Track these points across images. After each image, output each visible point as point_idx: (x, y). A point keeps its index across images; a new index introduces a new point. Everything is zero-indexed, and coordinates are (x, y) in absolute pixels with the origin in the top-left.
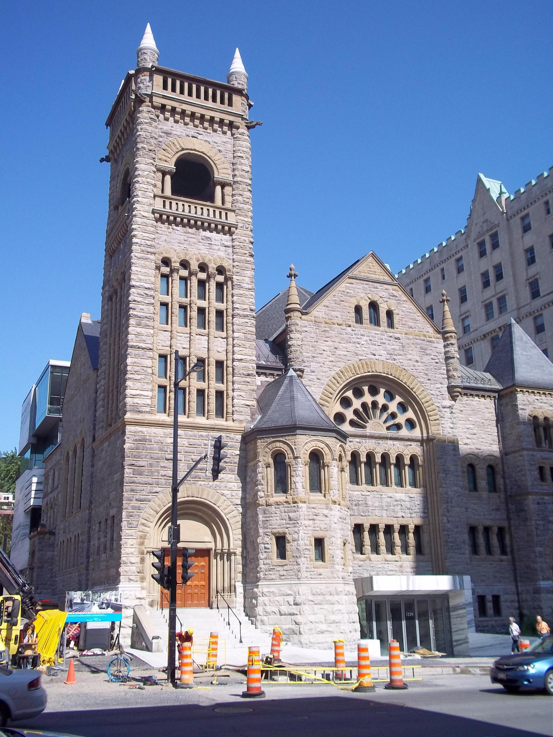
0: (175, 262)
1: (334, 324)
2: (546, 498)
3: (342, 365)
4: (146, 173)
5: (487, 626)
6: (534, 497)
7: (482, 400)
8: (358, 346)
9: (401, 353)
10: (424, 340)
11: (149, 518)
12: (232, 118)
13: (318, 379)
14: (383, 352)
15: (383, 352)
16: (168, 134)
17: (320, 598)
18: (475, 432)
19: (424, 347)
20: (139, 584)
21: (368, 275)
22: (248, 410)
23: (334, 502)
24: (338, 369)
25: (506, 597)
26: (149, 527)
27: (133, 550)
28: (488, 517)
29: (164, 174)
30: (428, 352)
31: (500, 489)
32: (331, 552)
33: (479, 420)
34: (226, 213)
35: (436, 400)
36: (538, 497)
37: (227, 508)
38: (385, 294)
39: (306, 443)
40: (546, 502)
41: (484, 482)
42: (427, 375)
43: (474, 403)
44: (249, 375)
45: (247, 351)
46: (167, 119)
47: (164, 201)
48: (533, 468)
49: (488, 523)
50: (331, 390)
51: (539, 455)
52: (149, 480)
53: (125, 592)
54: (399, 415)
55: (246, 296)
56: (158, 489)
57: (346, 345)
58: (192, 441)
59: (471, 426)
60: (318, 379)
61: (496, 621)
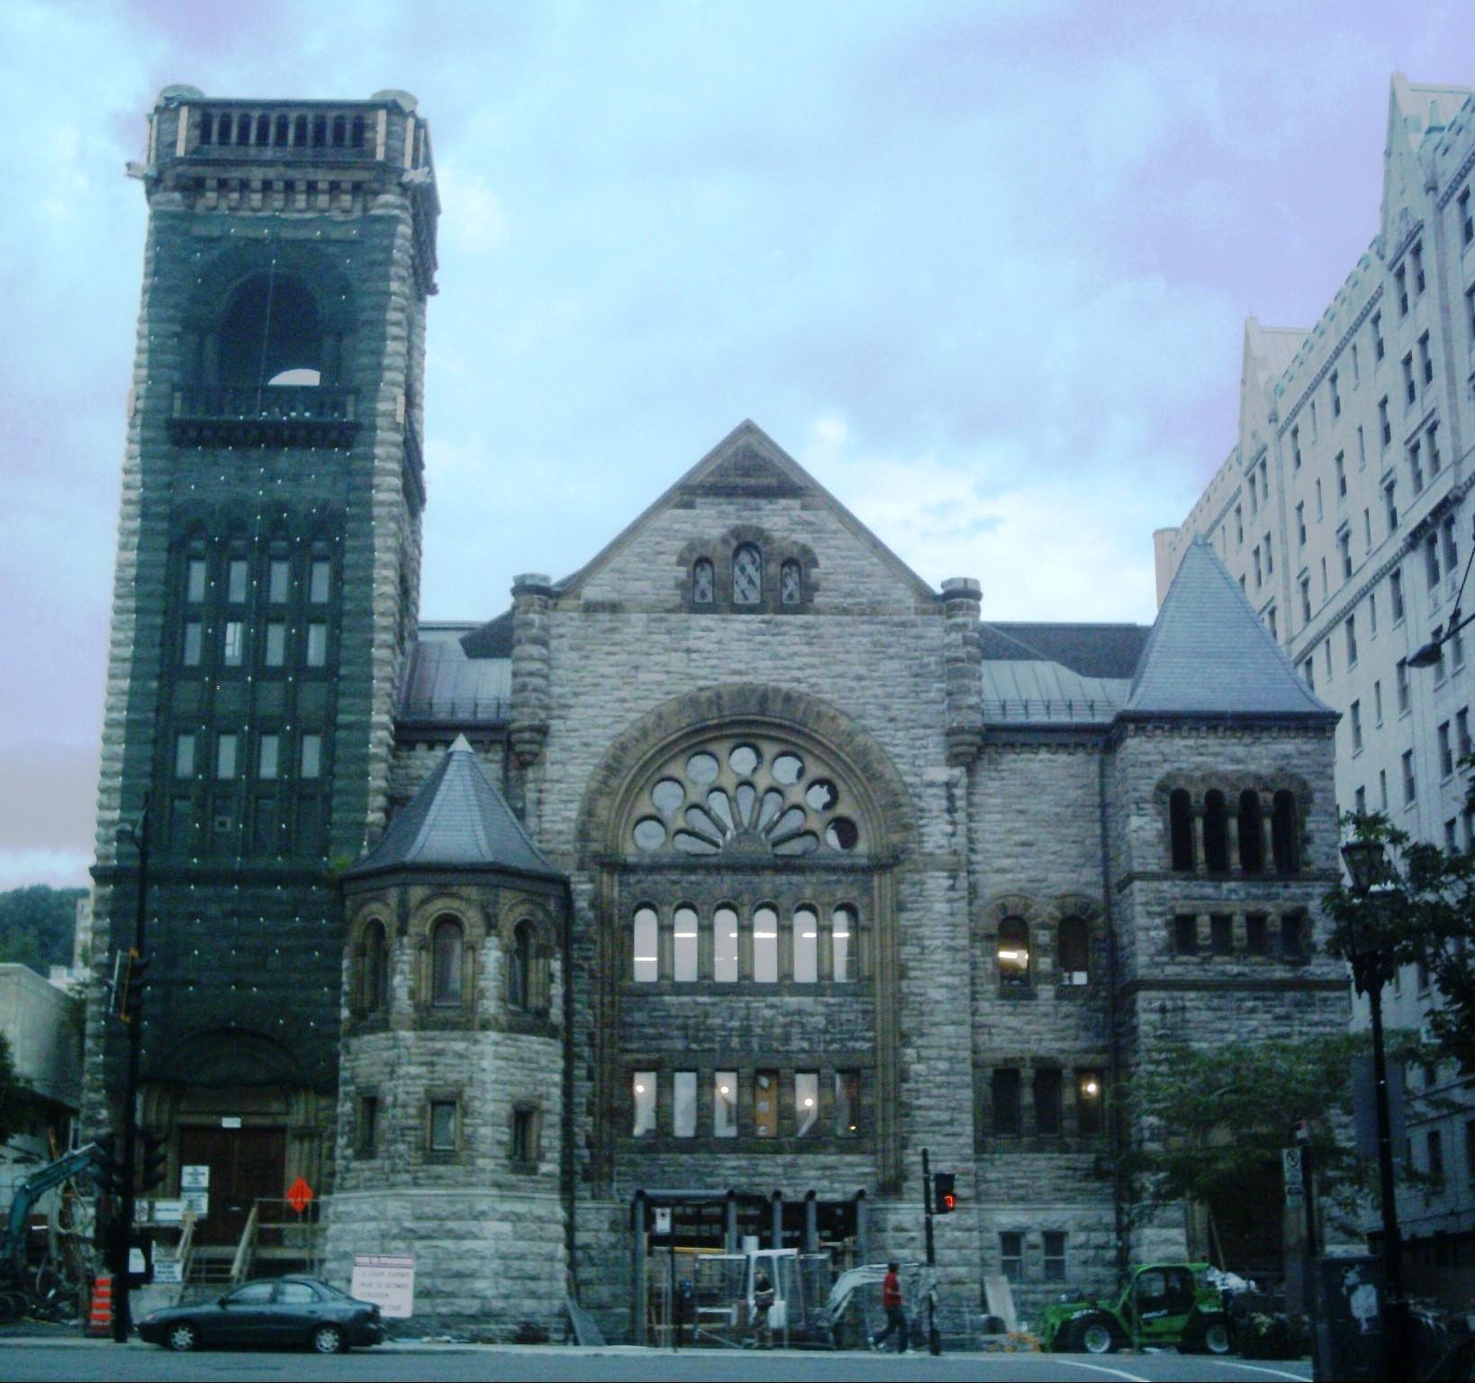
2: (1192, 995)
6: (1154, 994)
7: (1063, 758)
13: (586, 745)
17: (433, 1225)
18: (1030, 838)
19: (885, 639)
25: (1082, 1237)
30: (891, 651)
33: (1045, 807)
36: (1162, 994)
40: (1188, 1004)
42: (886, 708)
43: (1037, 765)
57: (664, 658)
61: (1048, 1292)
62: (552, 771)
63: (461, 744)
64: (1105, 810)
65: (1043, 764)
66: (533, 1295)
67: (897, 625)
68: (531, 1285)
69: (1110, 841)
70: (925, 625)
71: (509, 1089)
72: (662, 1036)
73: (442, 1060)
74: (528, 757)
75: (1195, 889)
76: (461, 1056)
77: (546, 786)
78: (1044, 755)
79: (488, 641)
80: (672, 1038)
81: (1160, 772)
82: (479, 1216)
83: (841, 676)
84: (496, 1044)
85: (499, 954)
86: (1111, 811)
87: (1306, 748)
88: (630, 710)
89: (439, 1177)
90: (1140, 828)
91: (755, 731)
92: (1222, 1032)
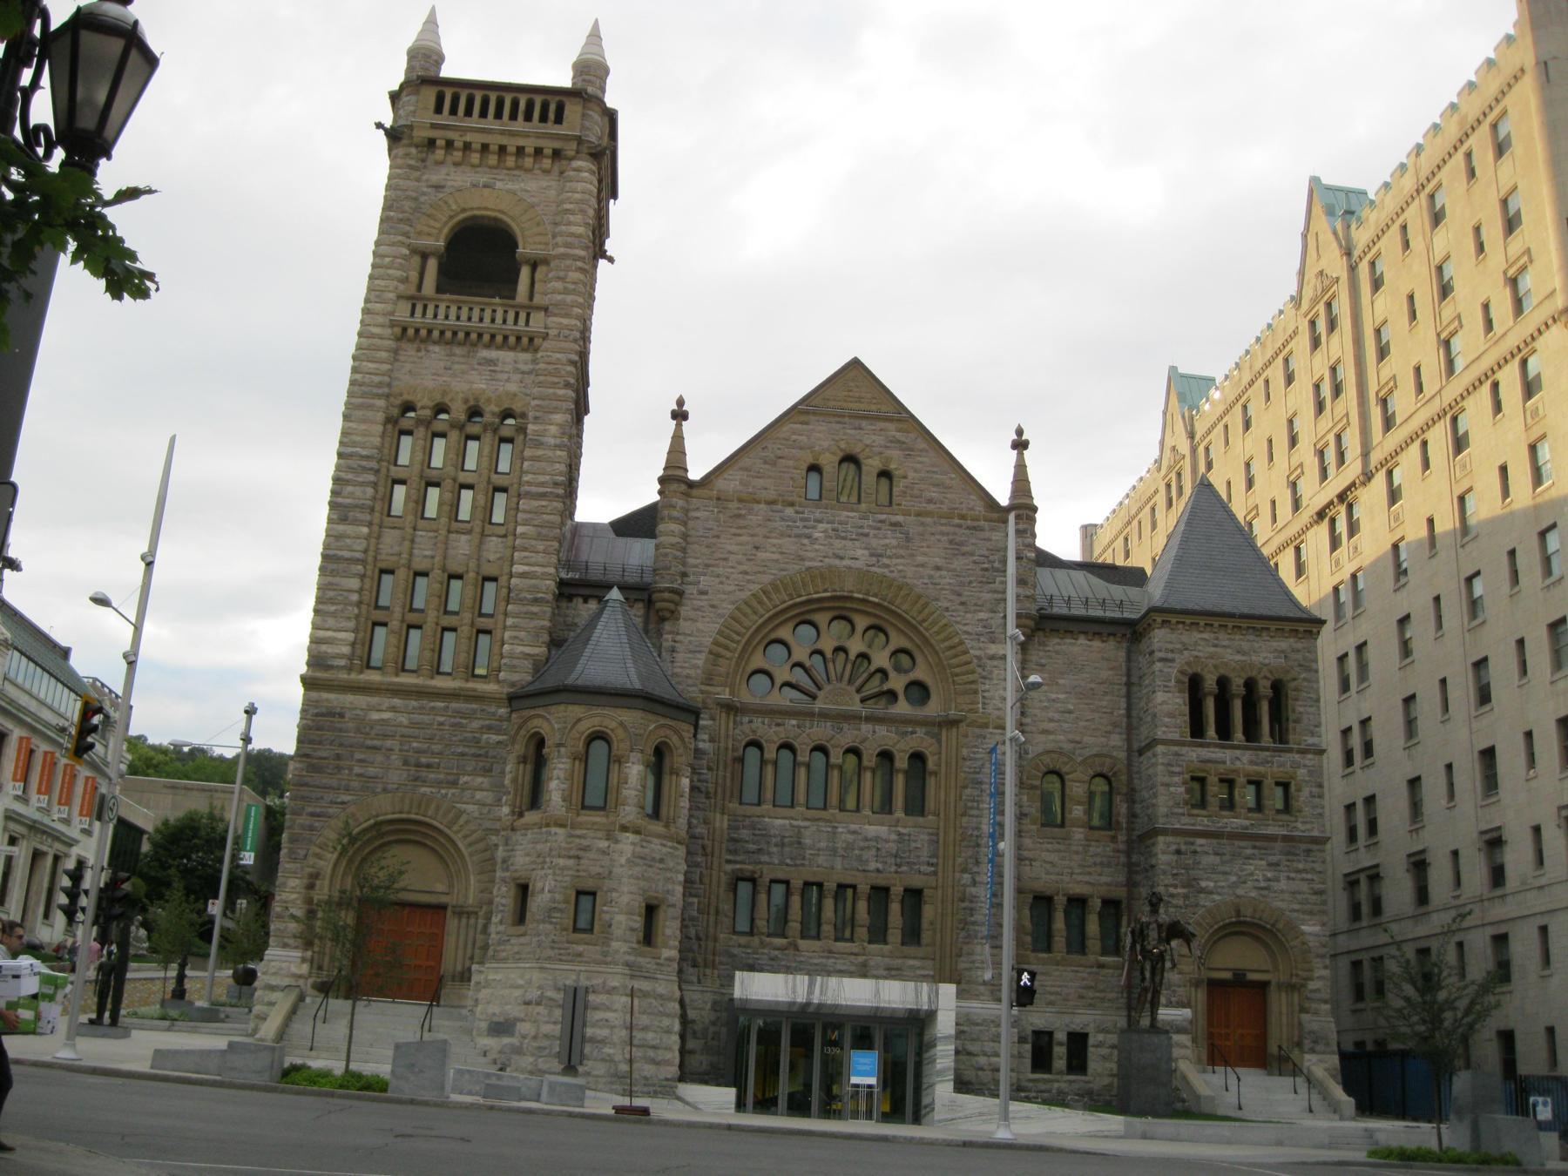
0: (423, 408)
1: (758, 502)
2: (1200, 841)
3: (767, 579)
4: (387, 260)
5: (1049, 1091)
6: (1170, 839)
7: (1097, 644)
8: (806, 541)
9: (902, 552)
10: (960, 526)
12: (557, 145)
13: (713, 606)
14: (859, 552)
15: (859, 552)
16: (438, 187)
19: (958, 539)
21: (845, 405)
22: (528, 665)
23: (624, 829)
24: (756, 588)
25: (1101, 1037)
27: (294, 896)
28: (1080, 878)
29: (424, 256)
30: (964, 549)
31: (1118, 822)
32: (607, 917)
34: (528, 315)
35: (975, 644)
36: (1178, 839)
38: (879, 440)
39: (579, 720)
41: (1080, 808)
42: (959, 595)
43: (1076, 649)
44: (536, 601)
45: (540, 558)
46: (441, 163)
47: (414, 307)
48: (1176, 779)
49: (1078, 890)
50: (737, 627)
51: (1194, 754)
52: (334, 783)
54: (892, 674)
55: (551, 461)
56: (347, 798)
58: (417, 718)
59: (1062, 696)
60: (713, 606)
62: (684, 625)
63: (615, 594)
64: (1131, 685)
65: (1080, 647)
66: (656, 1063)
67: (968, 528)
68: (651, 1053)
69: (1134, 713)
70: (992, 529)
71: (642, 883)
72: (760, 851)
73: (588, 854)
74: (667, 614)
75: (1205, 753)
76: (604, 852)
77: (678, 638)
78: (1082, 640)
79: (637, 525)
80: (769, 853)
81: (1180, 660)
82: (611, 991)
83: (922, 565)
84: (633, 844)
85: (641, 767)
86: (1135, 689)
87: (1299, 646)
88: (749, 581)
89: (580, 955)
90: (1164, 702)
91: (848, 605)
92: (1225, 873)
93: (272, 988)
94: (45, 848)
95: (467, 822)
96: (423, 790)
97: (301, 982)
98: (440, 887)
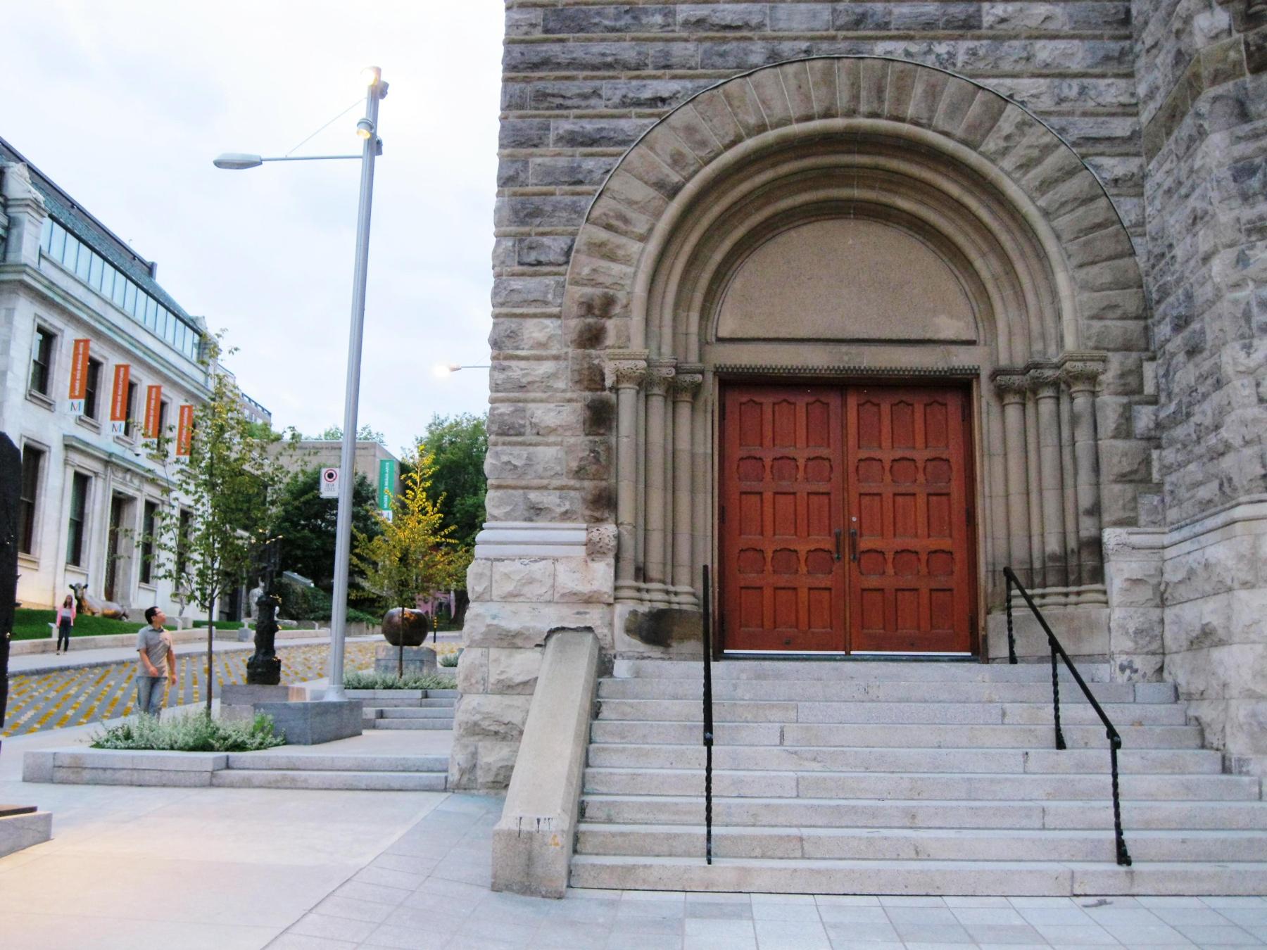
11: (626, 221)
20: (576, 533)
26: (626, 261)
27: (547, 367)
37: (1037, 161)
52: (627, 51)
53: (501, 568)
56: (665, 87)
93: (510, 640)
94: (130, 492)
95: (1022, 126)
96: (880, 48)
97: (594, 617)
98: (948, 327)
